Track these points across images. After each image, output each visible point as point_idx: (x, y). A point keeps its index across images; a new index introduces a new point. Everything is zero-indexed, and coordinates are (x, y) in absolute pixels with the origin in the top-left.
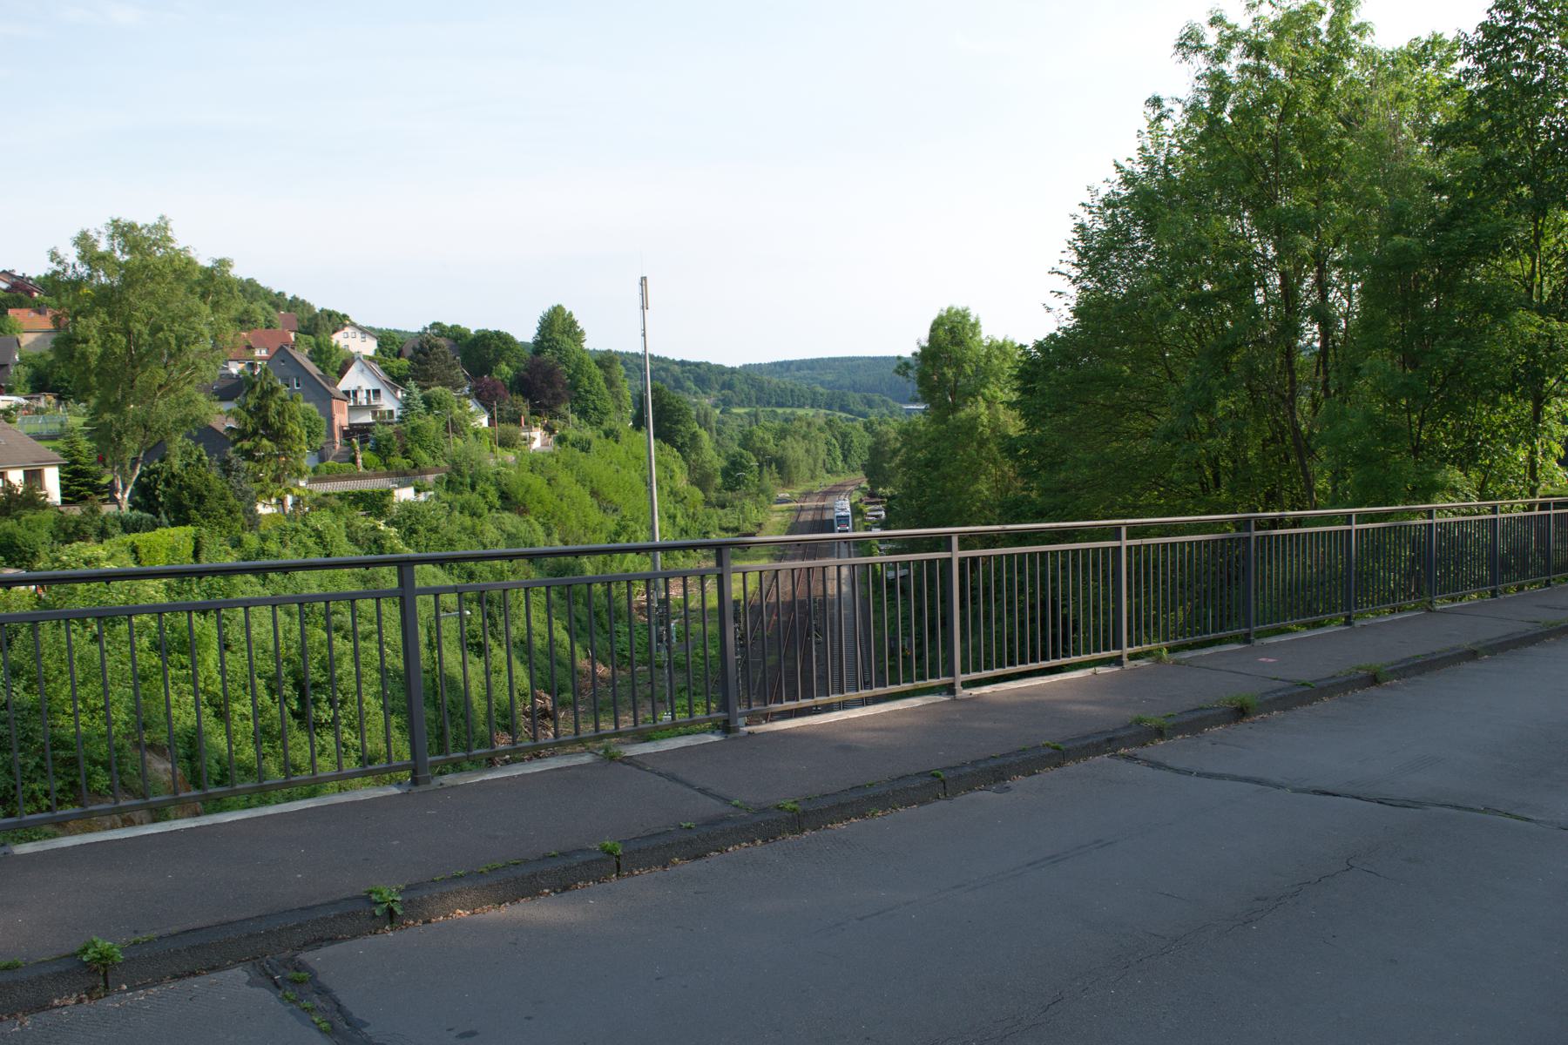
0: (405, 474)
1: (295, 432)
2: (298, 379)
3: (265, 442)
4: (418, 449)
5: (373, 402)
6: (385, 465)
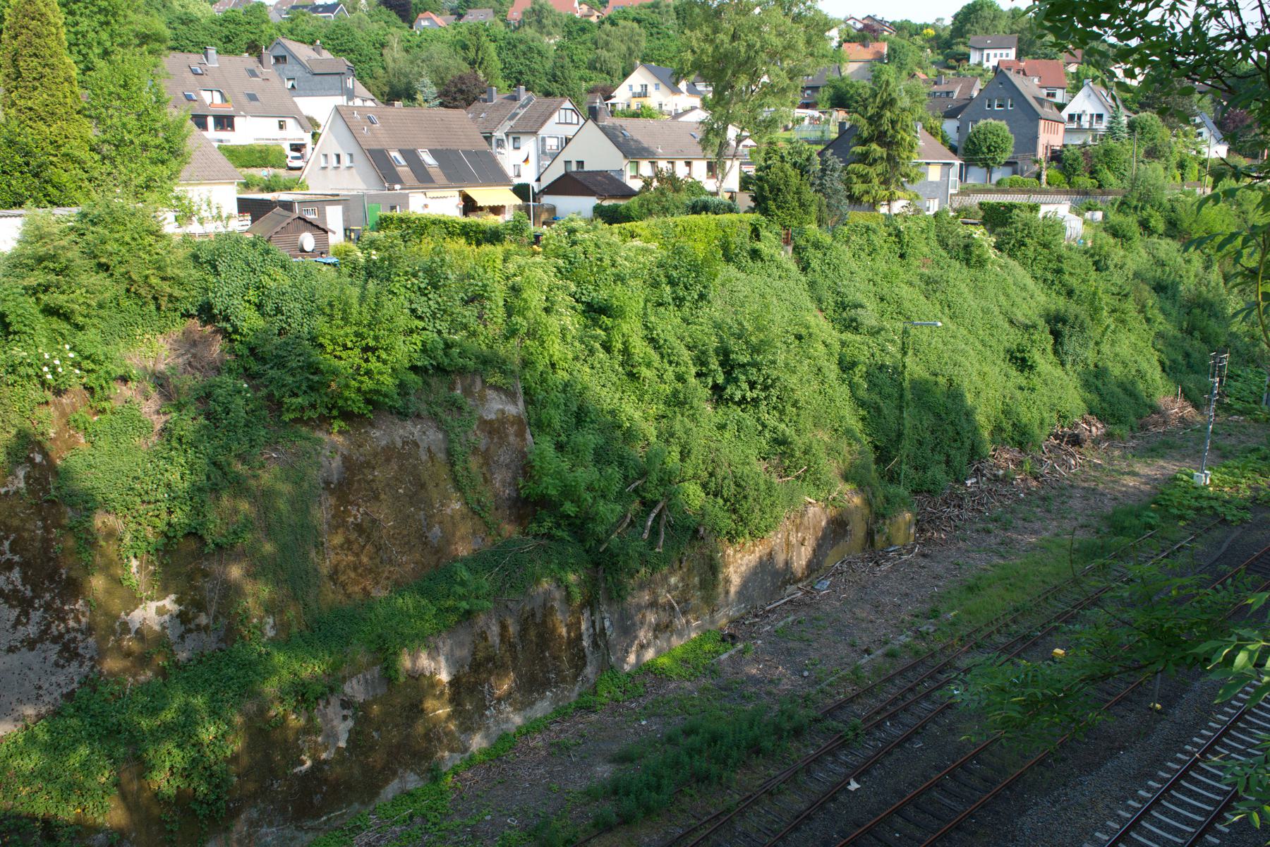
0: (1086, 193)
1: (905, 140)
2: (1012, 100)
3: (874, 146)
4: (1106, 171)
5: (1095, 126)
6: (1069, 183)
